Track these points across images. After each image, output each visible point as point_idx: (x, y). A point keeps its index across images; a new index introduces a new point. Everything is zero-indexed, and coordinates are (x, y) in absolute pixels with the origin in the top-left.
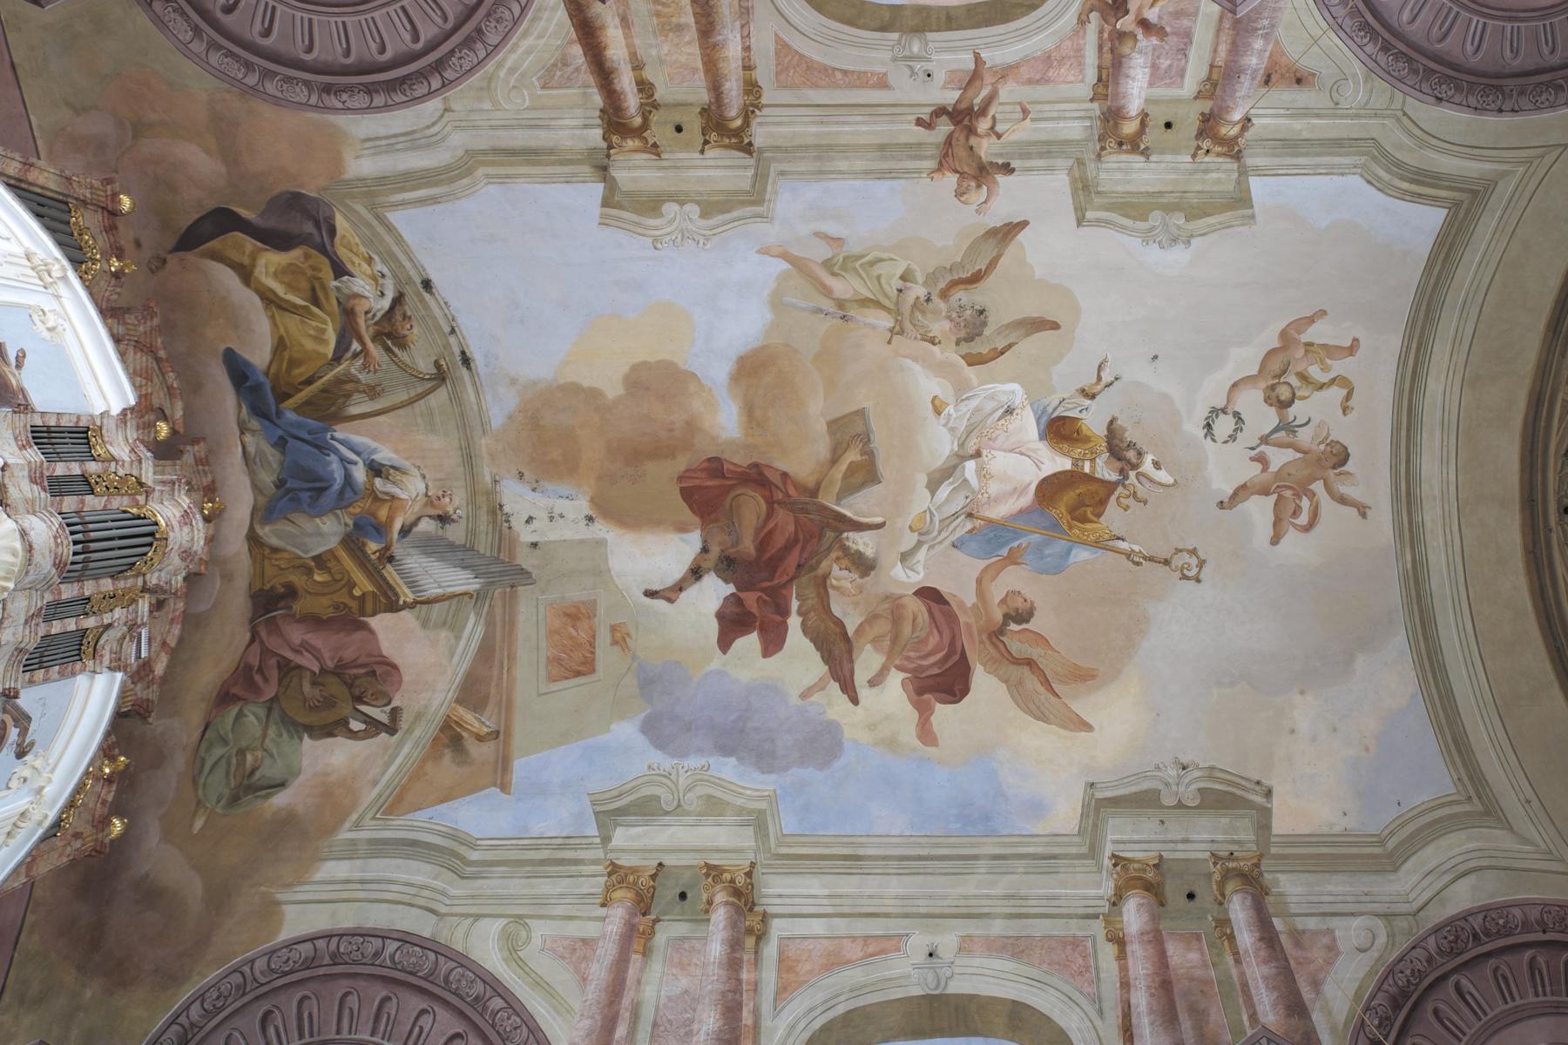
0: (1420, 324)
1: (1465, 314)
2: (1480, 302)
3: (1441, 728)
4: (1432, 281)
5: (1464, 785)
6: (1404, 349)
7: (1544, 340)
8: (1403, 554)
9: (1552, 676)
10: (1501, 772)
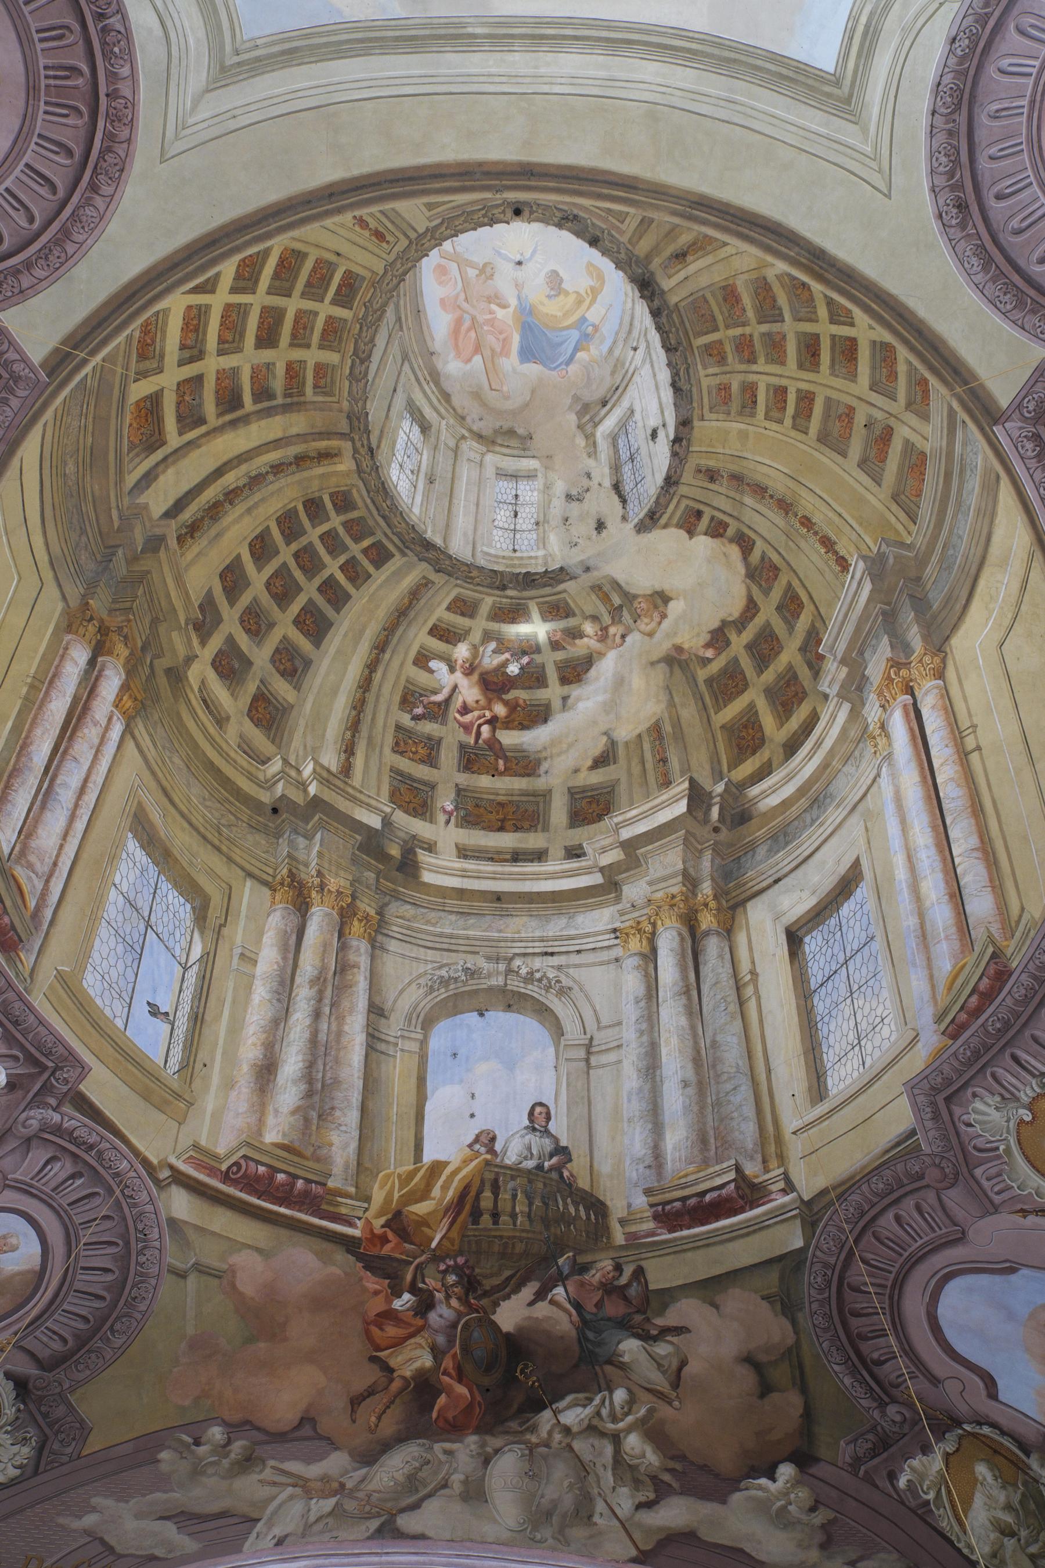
0: (716, 51)
1: (722, 103)
2: (736, 120)
3: (307, 36)
4: (759, 63)
5: (250, 50)
6: (691, 34)
7: (688, 192)
8: (483, 24)
9: (356, 172)
10: (263, 95)
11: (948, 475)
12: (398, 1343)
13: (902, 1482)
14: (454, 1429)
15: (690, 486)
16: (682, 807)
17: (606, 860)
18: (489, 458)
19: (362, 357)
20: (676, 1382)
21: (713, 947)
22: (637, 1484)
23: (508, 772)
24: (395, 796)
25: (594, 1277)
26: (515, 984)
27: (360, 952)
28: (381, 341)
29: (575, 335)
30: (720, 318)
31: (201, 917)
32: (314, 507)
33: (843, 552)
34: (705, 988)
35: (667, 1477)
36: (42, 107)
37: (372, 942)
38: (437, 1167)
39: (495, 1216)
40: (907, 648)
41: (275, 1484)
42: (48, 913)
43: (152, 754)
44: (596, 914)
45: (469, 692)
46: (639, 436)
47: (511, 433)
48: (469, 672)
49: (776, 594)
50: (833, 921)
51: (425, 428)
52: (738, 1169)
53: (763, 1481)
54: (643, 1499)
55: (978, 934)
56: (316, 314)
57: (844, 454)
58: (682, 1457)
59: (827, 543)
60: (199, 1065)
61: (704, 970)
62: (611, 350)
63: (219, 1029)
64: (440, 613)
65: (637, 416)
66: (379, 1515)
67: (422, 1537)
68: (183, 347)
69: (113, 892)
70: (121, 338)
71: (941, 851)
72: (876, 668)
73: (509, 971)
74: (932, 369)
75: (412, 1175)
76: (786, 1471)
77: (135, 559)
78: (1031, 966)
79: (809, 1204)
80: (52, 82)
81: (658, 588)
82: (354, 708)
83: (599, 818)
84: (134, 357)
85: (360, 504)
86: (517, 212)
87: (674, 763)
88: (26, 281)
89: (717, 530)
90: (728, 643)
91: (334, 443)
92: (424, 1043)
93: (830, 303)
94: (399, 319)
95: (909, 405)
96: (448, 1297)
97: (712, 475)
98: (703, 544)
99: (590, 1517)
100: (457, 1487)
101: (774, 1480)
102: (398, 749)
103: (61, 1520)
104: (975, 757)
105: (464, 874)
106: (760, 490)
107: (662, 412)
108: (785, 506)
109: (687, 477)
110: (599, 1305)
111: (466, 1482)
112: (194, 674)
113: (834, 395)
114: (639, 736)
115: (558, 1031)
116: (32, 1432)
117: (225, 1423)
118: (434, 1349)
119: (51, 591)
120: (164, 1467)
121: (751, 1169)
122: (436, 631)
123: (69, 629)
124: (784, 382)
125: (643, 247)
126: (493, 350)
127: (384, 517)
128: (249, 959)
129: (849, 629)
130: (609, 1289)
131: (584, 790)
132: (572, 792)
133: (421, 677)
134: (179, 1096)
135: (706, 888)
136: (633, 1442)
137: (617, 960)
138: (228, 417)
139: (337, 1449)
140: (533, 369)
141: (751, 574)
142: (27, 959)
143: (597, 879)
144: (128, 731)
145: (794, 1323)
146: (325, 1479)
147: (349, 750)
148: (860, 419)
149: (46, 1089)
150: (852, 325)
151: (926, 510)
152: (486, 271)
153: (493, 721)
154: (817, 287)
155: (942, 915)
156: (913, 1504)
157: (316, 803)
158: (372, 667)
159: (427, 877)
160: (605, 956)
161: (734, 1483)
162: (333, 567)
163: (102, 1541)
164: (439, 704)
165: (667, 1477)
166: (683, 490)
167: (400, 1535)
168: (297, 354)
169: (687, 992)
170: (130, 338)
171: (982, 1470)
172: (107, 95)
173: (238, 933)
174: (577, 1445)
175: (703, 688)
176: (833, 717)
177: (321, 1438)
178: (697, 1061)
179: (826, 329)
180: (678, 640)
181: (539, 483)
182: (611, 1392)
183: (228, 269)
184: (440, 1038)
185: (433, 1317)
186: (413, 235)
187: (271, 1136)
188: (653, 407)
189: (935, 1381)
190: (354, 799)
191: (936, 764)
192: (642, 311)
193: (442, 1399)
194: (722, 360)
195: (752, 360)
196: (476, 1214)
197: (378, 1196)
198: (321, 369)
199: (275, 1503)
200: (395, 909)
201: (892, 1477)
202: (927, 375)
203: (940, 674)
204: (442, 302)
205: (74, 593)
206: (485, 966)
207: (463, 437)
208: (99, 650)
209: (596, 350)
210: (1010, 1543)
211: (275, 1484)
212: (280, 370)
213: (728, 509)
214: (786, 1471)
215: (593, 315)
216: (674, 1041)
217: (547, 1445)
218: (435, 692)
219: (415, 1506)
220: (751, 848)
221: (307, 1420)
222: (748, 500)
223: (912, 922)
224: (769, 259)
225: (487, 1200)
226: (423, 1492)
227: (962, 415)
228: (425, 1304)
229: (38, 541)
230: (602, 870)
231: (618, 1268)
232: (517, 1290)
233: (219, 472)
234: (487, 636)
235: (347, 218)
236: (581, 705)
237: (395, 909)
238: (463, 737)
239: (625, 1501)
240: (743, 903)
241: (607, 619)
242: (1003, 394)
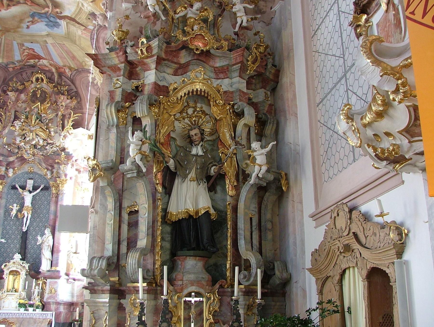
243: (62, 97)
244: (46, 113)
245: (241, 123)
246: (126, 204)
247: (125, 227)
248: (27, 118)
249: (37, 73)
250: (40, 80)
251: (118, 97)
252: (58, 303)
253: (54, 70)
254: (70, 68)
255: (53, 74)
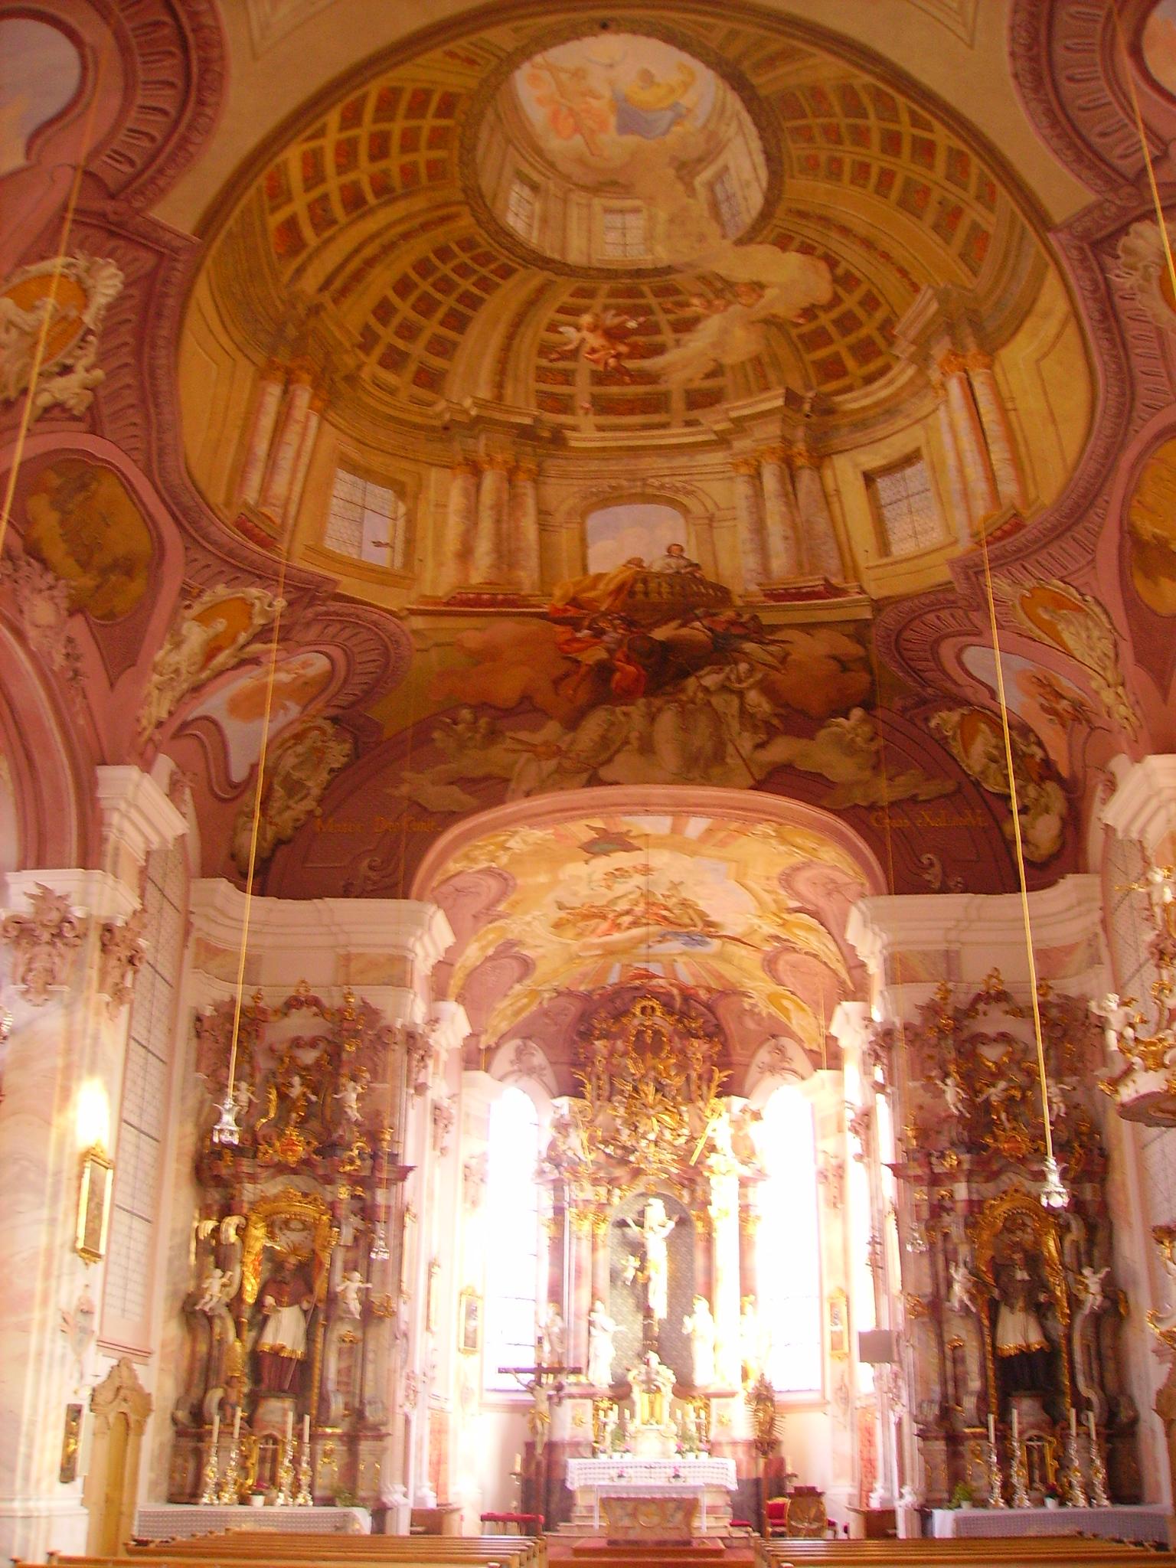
11: (1006, 256)
12: (580, 650)
13: (933, 724)
14: (627, 696)
15: (781, 219)
16: (780, 402)
17: (718, 427)
18: (598, 203)
19: (468, 149)
20: (783, 660)
21: (806, 478)
22: (755, 728)
23: (634, 382)
24: (540, 406)
25: (722, 618)
26: (649, 491)
27: (527, 489)
28: (484, 134)
29: (669, 115)
30: (808, 111)
31: (401, 492)
32: (443, 253)
33: (915, 280)
34: (801, 495)
35: (775, 722)
36: (139, 59)
37: (535, 481)
38: (600, 577)
39: (646, 594)
40: (964, 348)
41: (514, 751)
42: (291, 521)
43: (342, 423)
44: (712, 455)
45: (594, 340)
46: (732, 184)
47: (614, 183)
48: (593, 329)
49: (859, 293)
50: (898, 475)
51: (535, 188)
52: (826, 580)
53: (841, 720)
54: (759, 741)
55: (1006, 502)
56: (419, 128)
57: (919, 217)
58: (787, 705)
59: (903, 272)
60: (416, 562)
61: (797, 485)
62: (705, 126)
63: (426, 544)
64: (565, 299)
65: (732, 171)
66: (586, 770)
67: (617, 783)
68: (306, 179)
69: (334, 501)
70: (252, 192)
71: (981, 453)
72: (940, 349)
73: (645, 485)
74: (1000, 179)
75: (580, 582)
76: (857, 713)
77: (303, 323)
78: (1040, 527)
79: (876, 601)
80: (143, 39)
81: (755, 279)
82: (499, 362)
83: (711, 405)
84: (265, 198)
85: (482, 242)
86: (605, 26)
87: (772, 376)
88: (161, 182)
89: (806, 250)
90: (816, 317)
91: (453, 210)
92: (582, 524)
93: (913, 114)
94: (498, 117)
95: (978, 198)
96: (615, 628)
97: (802, 215)
98: (793, 258)
99: (723, 759)
100: (635, 743)
101: (847, 719)
102: (539, 379)
103: (388, 791)
104: (1012, 415)
105: (603, 439)
106: (845, 230)
107: (755, 169)
108: (868, 244)
109: (780, 211)
110: (727, 629)
111: (640, 738)
112: (365, 374)
113: (915, 177)
114: (743, 363)
115: (685, 511)
116: (348, 736)
117: (470, 706)
118: (608, 650)
119: (243, 362)
120: (439, 745)
121: (835, 581)
122: (561, 310)
123: (263, 378)
124: (867, 160)
125: (732, 53)
126: (593, 132)
127: (506, 249)
128: (442, 506)
129: (918, 326)
130: (732, 623)
131: (698, 391)
132: (688, 392)
133: (553, 337)
134: (404, 578)
135: (801, 447)
136: (753, 696)
137: (730, 478)
138: (355, 215)
139: (551, 718)
140: (631, 140)
141: (836, 280)
142: (283, 547)
143: (713, 437)
144: (323, 418)
145: (865, 648)
146: (546, 743)
147: (500, 386)
148: (936, 195)
149: (314, 598)
150: (931, 131)
151: (986, 269)
152: (578, 74)
153: (618, 356)
154: (901, 100)
155: (980, 487)
156: (937, 737)
157: (478, 419)
158: (510, 337)
159: (573, 444)
160: (721, 476)
161: (820, 722)
162: (467, 285)
163: (420, 805)
164: (571, 351)
165: (775, 722)
166: (775, 222)
167: (602, 783)
168: (408, 158)
169: (786, 495)
170: (259, 191)
171: (983, 726)
172: (193, 30)
173: (432, 494)
174: (715, 700)
175: (795, 339)
176: (903, 371)
177: (536, 709)
178: (794, 527)
179: (906, 128)
180: (774, 311)
181: (645, 214)
182: (736, 663)
183: (333, 118)
184: (594, 520)
185: (605, 638)
186: (503, 55)
187: (477, 577)
188: (746, 164)
189: (955, 683)
190: (507, 412)
191: (982, 411)
192: (734, 102)
193: (618, 676)
194: (810, 139)
195: (839, 141)
196: (632, 594)
197: (558, 592)
198: (431, 165)
199: (517, 768)
200: (548, 463)
201: (927, 720)
202: (995, 181)
203: (989, 367)
204: (540, 101)
205: (260, 358)
206: (625, 483)
207: (571, 190)
208: (289, 382)
209: (692, 125)
210: (994, 766)
211: (514, 751)
212: (395, 173)
213: (818, 239)
214: (857, 713)
215: (687, 100)
216: (777, 518)
217: (693, 702)
218: (566, 344)
219: (610, 760)
220: (837, 428)
221: (526, 698)
222: (834, 235)
223: (958, 486)
224: (856, 72)
225: (640, 587)
226: (613, 748)
227: (1021, 218)
228: (599, 633)
229: (224, 340)
230: (715, 432)
231: (739, 615)
232: (666, 623)
233: (357, 251)
234: (606, 308)
235: (438, 53)
236: (692, 345)
237: (548, 463)
238: (594, 367)
239: (746, 742)
240: (829, 455)
241: (711, 296)
242: (1058, 216)
243: (696, 1043)
244: (669, 1076)
245: (1069, 1238)
246: (947, 1337)
247: (949, 1364)
248: (636, 1089)
249: (644, 997)
250: (649, 1011)
251: (925, 1213)
252: (734, 1443)
253: (675, 991)
254: (709, 990)
255: (672, 996)
